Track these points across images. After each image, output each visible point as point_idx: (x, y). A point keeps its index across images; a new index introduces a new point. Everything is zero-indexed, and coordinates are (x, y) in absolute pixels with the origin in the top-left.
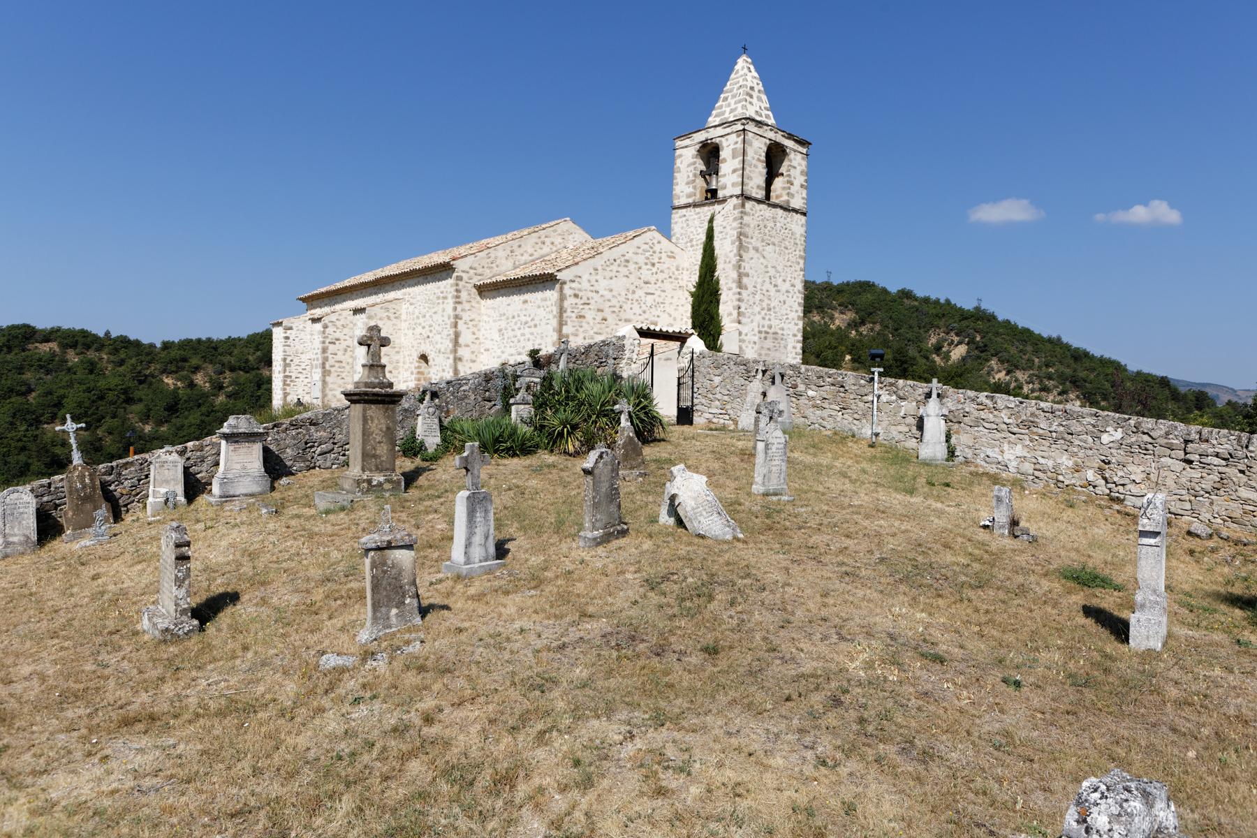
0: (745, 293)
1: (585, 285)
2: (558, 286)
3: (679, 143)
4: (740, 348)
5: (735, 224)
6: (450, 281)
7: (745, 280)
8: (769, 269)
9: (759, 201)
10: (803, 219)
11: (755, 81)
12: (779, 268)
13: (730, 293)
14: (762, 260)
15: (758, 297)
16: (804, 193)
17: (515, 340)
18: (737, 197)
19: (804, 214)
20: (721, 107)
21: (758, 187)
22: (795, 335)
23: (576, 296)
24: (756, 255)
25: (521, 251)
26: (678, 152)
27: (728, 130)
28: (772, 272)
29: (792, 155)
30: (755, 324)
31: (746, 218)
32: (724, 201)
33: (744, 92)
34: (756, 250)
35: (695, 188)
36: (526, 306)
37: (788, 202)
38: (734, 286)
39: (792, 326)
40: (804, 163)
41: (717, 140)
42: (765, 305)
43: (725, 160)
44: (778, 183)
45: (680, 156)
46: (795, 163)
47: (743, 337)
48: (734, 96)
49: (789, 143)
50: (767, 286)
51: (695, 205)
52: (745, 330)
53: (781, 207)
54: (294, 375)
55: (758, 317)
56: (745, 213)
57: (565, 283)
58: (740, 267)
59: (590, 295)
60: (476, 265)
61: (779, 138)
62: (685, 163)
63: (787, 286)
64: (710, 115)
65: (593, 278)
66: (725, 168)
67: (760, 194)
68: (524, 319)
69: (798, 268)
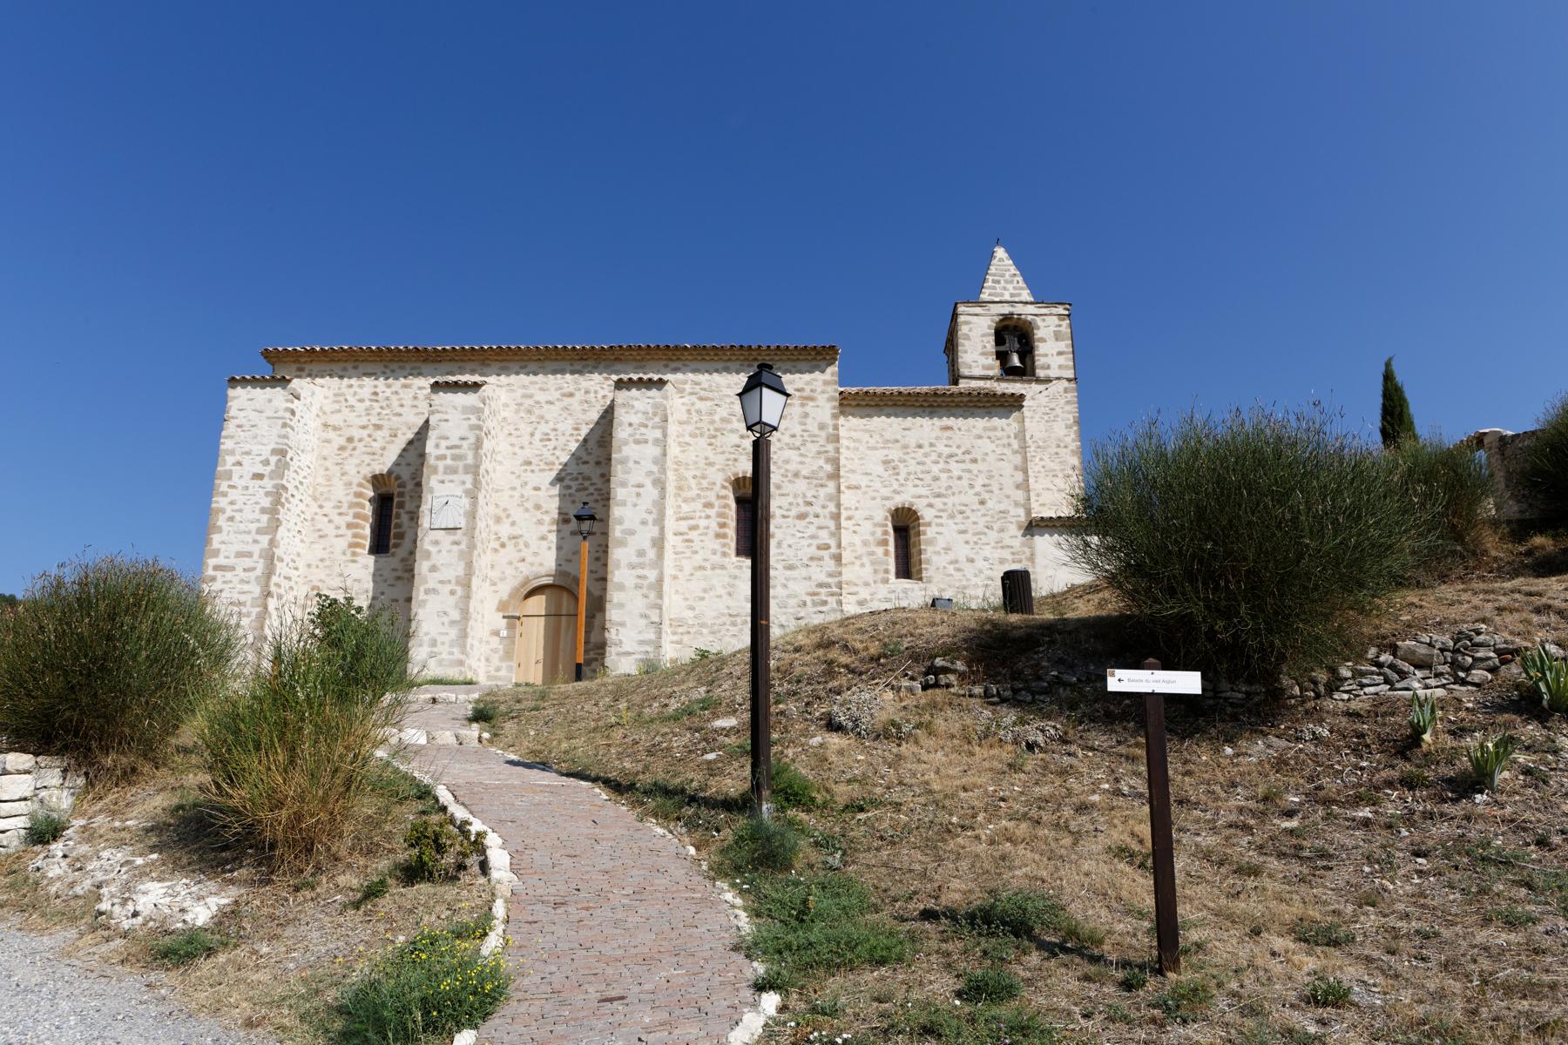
17: (928, 478)
18: (1069, 380)
32: (1048, 380)
33: (1006, 284)
36: (949, 433)
45: (967, 323)
54: (291, 490)
68: (947, 451)
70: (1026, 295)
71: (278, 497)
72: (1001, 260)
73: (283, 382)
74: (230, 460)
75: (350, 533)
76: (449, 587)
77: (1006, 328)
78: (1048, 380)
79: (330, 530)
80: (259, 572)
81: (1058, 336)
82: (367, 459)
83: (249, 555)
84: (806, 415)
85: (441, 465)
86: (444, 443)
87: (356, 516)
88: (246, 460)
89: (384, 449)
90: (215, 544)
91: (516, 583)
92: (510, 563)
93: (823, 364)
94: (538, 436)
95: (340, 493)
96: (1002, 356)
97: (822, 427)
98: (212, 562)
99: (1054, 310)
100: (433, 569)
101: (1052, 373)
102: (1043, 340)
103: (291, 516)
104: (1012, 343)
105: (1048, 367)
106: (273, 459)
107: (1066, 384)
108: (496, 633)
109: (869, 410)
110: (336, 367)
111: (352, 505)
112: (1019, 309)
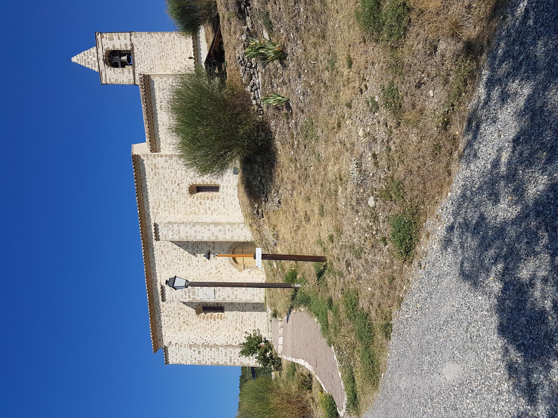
18: (131, 35)
26: (108, 82)
32: (132, 45)
33: (89, 59)
41: (104, 52)
45: (110, 80)
48: (88, 58)
64: (94, 71)
66: (118, 47)
70: (93, 50)
71: (205, 346)
72: (78, 60)
73: (166, 349)
74: (194, 361)
75: (217, 320)
76: (235, 291)
77: (110, 61)
78: (132, 45)
79: (217, 326)
80: (231, 349)
81: (111, 39)
82: (191, 316)
83: (226, 353)
84: (162, 167)
85: (192, 297)
86: (184, 296)
87: (211, 318)
88: (194, 357)
89: (187, 312)
90: (223, 363)
91: (232, 267)
92: (225, 269)
93: (140, 160)
94: (179, 262)
95: (204, 323)
96: (123, 65)
97: (166, 161)
98: (229, 363)
99: (99, 40)
100: (229, 297)
101: (129, 43)
102: (114, 46)
103: (212, 341)
104: (116, 59)
105: (126, 44)
106: (193, 348)
107: (133, 37)
108: (250, 272)
109: (157, 139)
110: (158, 329)
111: (207, 320)
112: (101, 56)
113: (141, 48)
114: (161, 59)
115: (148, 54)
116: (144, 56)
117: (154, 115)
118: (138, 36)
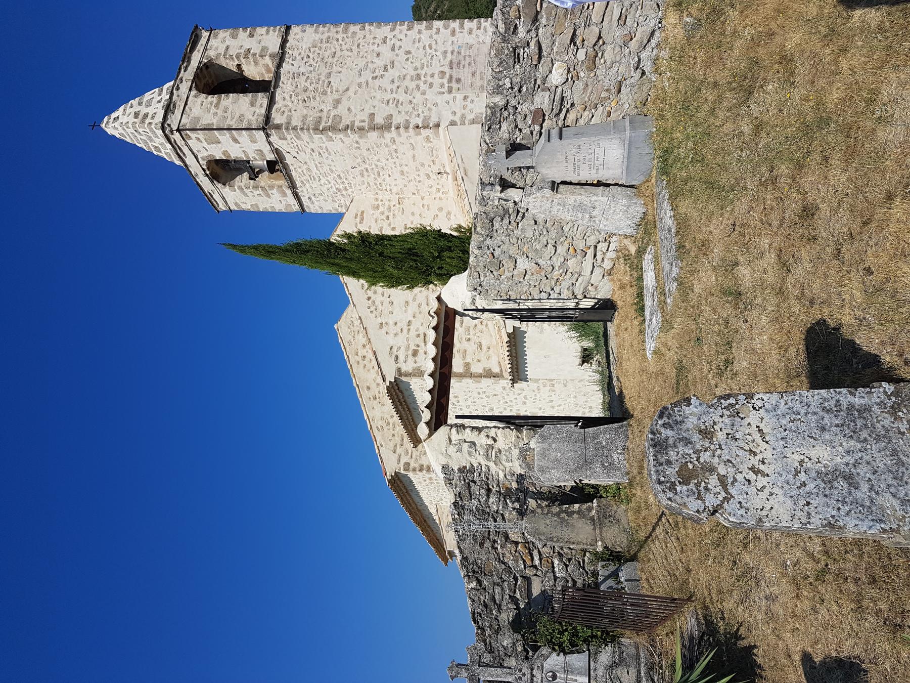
0: (398, 119)
1: (401, 341)
2: (404, 379)
3: (222, 207)
4: (473, 122)
5: (305, 136)
6: (411, 475)
7: (379, 120)
8: (362, 80)
9: (272, 102)
10: (295, 30)
11: (128, 111)
12: (361, 63)
13: (397, 139)
14: (351, 93)
15: (402, 97)
16: (261, 31)
18: (268, 136)
19: (288, 28)
20: (166, 153)
21: (253, 104)
22: (453, 33)
23: (415, 353)
24: (345, 103)
25: (373, 386)
26: (233, 207)
27: (185, 150)
28: (367, 75)
29: (211, 53)
30: (440, 99)
31: (294, 123)
32: (277, 151)
34: (337, 102)
35: (271, 187)
37: (272, 56)
38: (388, 135)
39: (439, 38)
40: (222, 34)
42: (412, 85)
43: (225, 153)
44: (252, 72)
45: (236, 204)
46: (223, 46)
47: (457, 119)
48: (151, 140)
49: (196, 59)
50: (385, 83)
51: (293, 186)
52: (447, 117)
53: (279, 66)
55: (430, 95)
56: (288, 123)
57: (399, 370)
58: (361, 129)
59: (413, 333)
60: (391, 445)
61: (188, 75)
62: (244, 199)
63: (385, 50)
65: (393, 330)
66: (236, 152)
67: (262, 99)
69: (360, 34)
101: (266, 149)
105: (261, 151)
107: (274, 138)
113: (301, 156)
114: (363, 176)
115: (326, 168)
116: (314, 170)
117: (412, 410)
118: (289, 137)
